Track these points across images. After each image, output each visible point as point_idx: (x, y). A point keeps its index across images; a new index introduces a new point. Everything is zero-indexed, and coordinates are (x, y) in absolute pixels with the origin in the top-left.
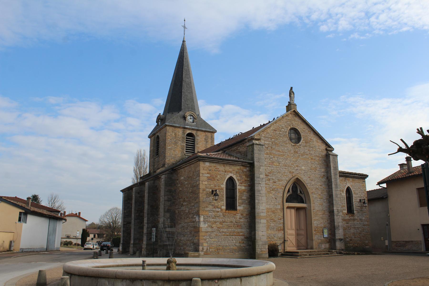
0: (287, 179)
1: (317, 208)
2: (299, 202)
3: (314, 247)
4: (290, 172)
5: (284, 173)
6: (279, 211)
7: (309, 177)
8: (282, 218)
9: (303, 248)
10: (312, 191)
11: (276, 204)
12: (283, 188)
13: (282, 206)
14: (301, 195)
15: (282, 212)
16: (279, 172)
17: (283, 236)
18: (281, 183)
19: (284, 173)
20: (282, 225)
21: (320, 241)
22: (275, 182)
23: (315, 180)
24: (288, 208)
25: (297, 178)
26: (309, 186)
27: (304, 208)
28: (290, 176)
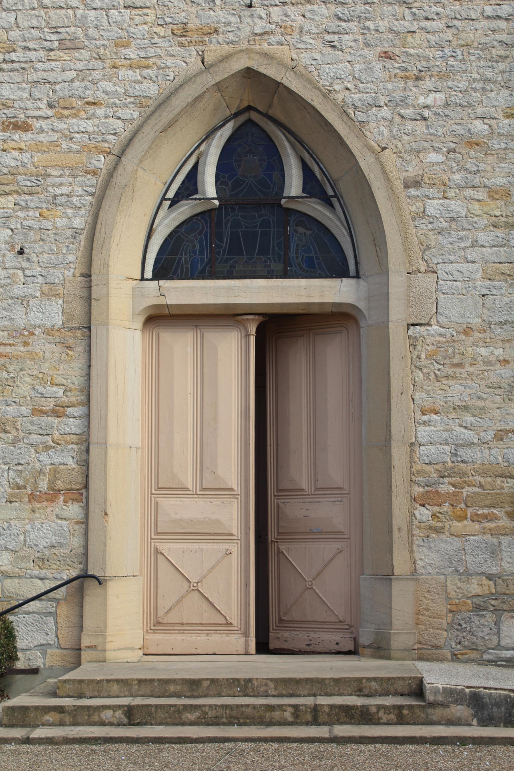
0: (152, 90)
1: (457, 310)
2: (310, 270)
3: (399, 640)
4: (182, 31)
5: (121, 43)
6: (42, 346)
7: (387, 56)
8: (76, 397)
9: (329, 638)
10: (412, 171)
11: (18, 290)
12: (101, 162)
13: (78, 308)
14: (315, 209)
15: (79, 350)
16: (70, 45)
17: (76, 542)
18: (89, 126)
19: (121, 43)
20: (68, 459)
21: (475, 587)
22: (26, 127)
23: (446, 75)
24: (158, 318)
25: (249, 73)
26: (378, 132)
27: (337, 319)
28: (180, 62)
